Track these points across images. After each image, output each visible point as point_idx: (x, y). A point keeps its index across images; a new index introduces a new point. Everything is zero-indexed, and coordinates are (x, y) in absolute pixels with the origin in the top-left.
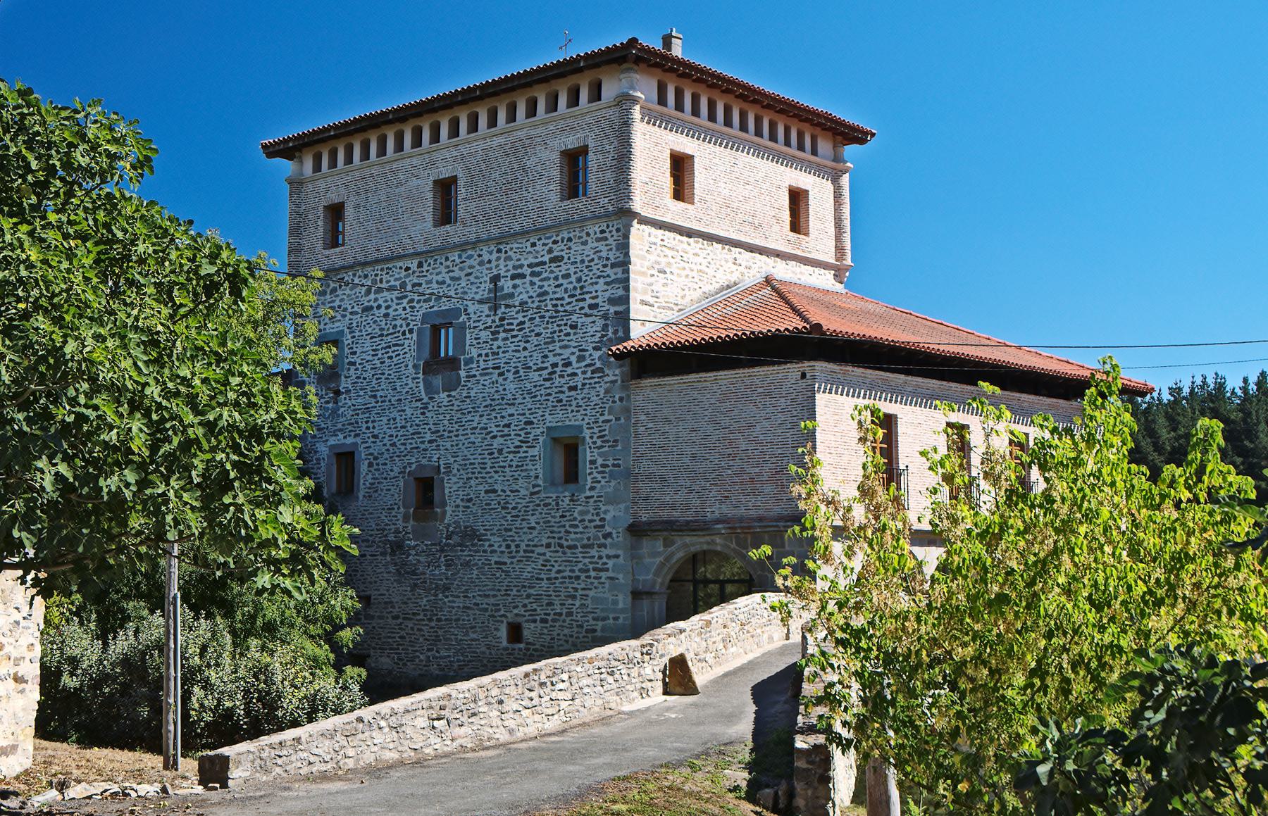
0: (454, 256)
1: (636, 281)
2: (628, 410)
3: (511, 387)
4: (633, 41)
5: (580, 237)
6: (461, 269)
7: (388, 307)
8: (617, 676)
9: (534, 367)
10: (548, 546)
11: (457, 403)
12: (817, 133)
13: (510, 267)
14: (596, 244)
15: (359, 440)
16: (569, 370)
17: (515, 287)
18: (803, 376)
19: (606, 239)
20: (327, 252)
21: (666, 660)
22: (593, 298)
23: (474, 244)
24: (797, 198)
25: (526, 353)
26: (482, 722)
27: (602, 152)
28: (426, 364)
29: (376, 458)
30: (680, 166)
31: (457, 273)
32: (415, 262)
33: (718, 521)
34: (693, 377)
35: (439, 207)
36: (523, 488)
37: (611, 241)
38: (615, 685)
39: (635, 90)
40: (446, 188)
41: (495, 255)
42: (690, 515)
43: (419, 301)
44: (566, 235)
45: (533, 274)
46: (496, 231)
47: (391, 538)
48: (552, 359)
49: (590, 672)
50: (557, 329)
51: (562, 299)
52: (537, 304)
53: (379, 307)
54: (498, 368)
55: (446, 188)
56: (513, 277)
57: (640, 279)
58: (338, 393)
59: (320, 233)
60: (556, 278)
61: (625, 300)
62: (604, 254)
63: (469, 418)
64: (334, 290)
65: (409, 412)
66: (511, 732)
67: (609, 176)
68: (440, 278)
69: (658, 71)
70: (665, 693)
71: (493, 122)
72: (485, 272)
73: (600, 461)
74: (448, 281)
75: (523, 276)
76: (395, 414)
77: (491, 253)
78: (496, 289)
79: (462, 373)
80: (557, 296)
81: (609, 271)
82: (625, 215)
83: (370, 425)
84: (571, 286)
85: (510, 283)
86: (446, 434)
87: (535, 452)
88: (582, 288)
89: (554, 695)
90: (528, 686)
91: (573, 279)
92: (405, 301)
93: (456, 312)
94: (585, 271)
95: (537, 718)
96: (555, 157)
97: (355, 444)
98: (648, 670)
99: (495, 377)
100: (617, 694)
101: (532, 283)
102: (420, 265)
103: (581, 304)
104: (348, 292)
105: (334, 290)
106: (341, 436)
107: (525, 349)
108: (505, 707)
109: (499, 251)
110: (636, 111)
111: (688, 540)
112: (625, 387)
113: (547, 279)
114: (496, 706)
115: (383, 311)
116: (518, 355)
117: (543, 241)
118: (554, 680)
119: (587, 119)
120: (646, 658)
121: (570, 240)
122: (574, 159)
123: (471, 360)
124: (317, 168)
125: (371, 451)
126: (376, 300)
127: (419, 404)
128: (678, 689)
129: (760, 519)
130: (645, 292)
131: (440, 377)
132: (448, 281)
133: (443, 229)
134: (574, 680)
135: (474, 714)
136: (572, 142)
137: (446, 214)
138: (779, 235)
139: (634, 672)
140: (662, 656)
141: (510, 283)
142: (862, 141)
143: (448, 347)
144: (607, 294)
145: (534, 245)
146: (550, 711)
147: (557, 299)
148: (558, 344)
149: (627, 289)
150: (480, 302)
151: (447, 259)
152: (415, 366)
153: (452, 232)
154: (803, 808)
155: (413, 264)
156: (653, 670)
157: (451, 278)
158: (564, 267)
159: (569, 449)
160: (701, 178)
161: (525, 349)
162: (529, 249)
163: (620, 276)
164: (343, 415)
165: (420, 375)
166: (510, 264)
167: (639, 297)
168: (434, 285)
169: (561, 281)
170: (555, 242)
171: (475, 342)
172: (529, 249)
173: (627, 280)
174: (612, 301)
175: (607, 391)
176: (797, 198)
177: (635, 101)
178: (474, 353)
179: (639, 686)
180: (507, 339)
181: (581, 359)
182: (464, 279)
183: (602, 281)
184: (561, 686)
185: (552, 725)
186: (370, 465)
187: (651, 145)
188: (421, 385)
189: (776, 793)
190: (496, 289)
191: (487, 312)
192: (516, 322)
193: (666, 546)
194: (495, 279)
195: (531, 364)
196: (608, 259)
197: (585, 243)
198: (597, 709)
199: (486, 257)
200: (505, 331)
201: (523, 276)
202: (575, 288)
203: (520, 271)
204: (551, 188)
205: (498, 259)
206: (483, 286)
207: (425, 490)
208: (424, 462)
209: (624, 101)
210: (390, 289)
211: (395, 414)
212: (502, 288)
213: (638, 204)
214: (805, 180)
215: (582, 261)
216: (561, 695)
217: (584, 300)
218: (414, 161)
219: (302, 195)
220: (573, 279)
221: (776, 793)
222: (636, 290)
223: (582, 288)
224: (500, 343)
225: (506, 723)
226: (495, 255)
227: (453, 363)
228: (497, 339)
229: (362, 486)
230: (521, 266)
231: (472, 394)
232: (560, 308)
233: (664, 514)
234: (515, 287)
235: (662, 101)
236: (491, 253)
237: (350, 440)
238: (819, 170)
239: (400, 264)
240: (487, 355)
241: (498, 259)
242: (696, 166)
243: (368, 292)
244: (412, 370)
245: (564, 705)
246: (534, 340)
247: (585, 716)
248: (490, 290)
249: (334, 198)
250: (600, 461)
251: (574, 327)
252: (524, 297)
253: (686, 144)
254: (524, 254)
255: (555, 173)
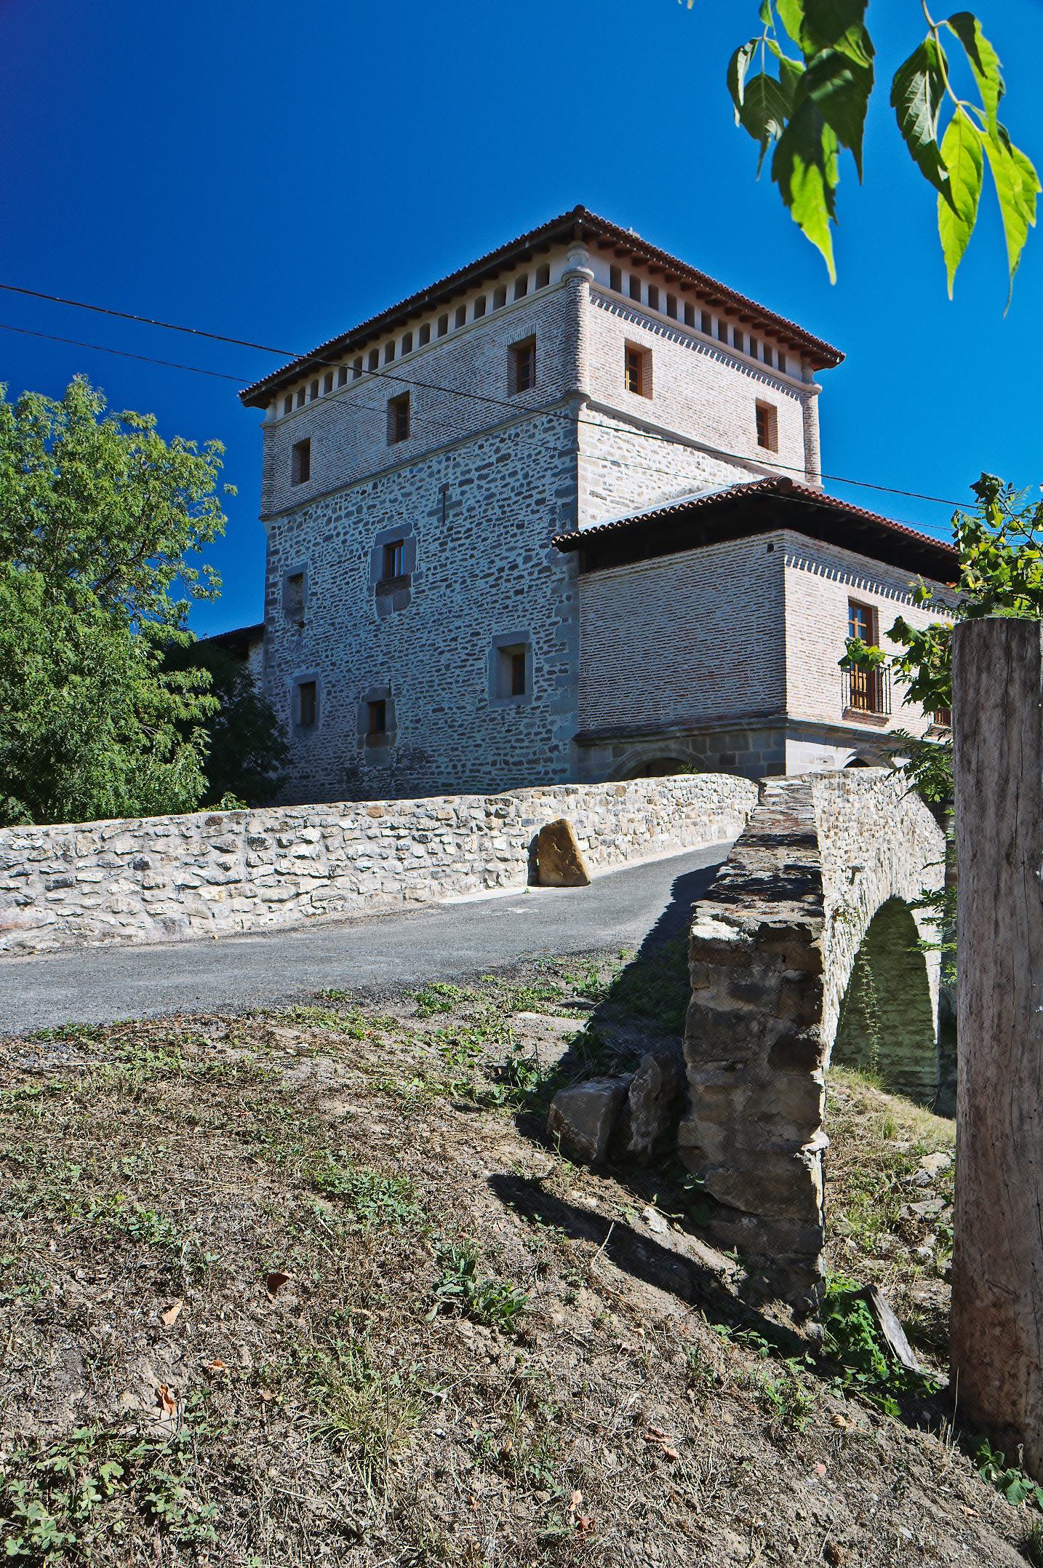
0: (406, 472)
1: (585, 469)
2: (575, 610)
3: (458, 598)
4: (580, 209)
5: (527, 431)
6: (412, 484)
7: (345, 534)
8: (435, 845)
9: (481, 575)
10: (494, 763)
11: (407, 621)
12: (786, 348)
13: (458, 474)
14: (543, 436)
15: (319, 670)
16: (516, 573)
17: (463, 493)
18: (770, 548)
19: (554, 428)
20: (294, 489)
21: (535, 830)
22: (540, 493)
23: (424, 456)
24: (765, 415)
25: (473, 561)
26: (88, 902)
27: (550, 339)
28: (380, 585)
29: (334, 686)
30: (637, 360)
31: (409, 488)
32: (371, 485)
33: (673, 724)
34: (645, 564)
35: (394, 427)
36: (469, 703)
37: (558, 429)
38: (428, 861)
39: (583, 266)
40: (400, 406)
41: (444, 464)
42: (642, 719)
43: (373, 523)
44: (513, 432)
45: (481, 477)
46: (445, 439)
47: (347, 765)
48: (499, 564)
49: (374, 831)
50: (503, 531)
51: (509, 498)
52: (484, 507)
53: (338, 534)
54: (446, 580)
55: (400, 406)
56: (461, 484)
57: (590, 468)
58: (302, 625)
59: (289, 473)
60: (503, 478)
61: (573, 490)
62: (551, 445)
63: (418, 635)
64: (301, 524)
65: (363, 636)
66: (169, 925)
67: (556, 362)
68: (392, 497)
69: (610, 253)
70: (535, 880)
71: (443, 330)
72: (435, 483)
73: (546, 668)
74: (400, 498)
75: (470, 481)
76: (351, 639)
77: (440, 463)
78: (445, 498)
79: (412, 590)
80: (504, 496)
81: (556, 461)
82: (574, 397)
83: (329, 653)
84: (518, 484)
85: (459, 490)
86: (397, 654)
87: (481, 664)
88: (529, 484)
89: (284, 865)
90: (218, 841)
91: (520, 476)
92: (361, 525)
93: (406, 529)
94: (533, 465)
95: (239, 903)
96: (502, 353)
97: (316, 674)
98: (500, 843)
99: (443, 590)
100: (434, 876)
101: (480, 487)
102: (375, 487)
103: (528, 501)
104: (311, 524)
105: (301, 524)
106: (304, 667)
107: (472, 556)
108: (152, 877)
109: (448, 459)
110: (585, 289)
111: (639, 747)
112: (573, 584)
113: (494, 480)
114: (129, 872)
115: (342, 538)
116: (465, 564)
117: (491, 441)
118: (285, 838)
119: (535, 307)
120: (496, 822)
121: (517, 435)
122: (523, 353)
123: (419, 576)
124: (288, 408)
125: (330, 678)
126: (336, 528)
127: (372, 627)
128: (554, 877)
129: (720, 718)
130: (596, 483)
131: (391, 597)
132: (400, 498)
133: (396, 446)
134: (334, 843)
135: (64, 884)
136: (519, 334)
137: (400, 431)
138: (746, 445)
139: (473, 841)
140: (527, 822)
141: (459, 490)
142: (832, 364)
143: (400, 568)
144: (555, 487)
145: (481, 447)
146: (274, 894)
147: (504, 500)
148: (505, 547)
149: (575, 478)
150: (430, 514)
151: (399, 476)
152: (369, 589)
153: (407, 448)
154: (715, 1156)
155: (368, 487)
156: (510, 843)
157: (404, 495)
158: (512, 465)
159: (514, 657)
160: (659, 374)
161: (472, 556)
162: (477, 451)
163: (568, 464)
164: (306, 646)
165: (374, 598)
166: (459, 470)
167: (590, 488)
168: (388, 504)
169: (508, 480)
170: (502, 441)
171: (424, 556)
172: (477, 451)
173: (576, 467)
174: (559, 493)
175: (554, 591)
176: (765, 415)
177: (584, 278)
178: (424, 567)
179: (479, 866)
180: (454, 549)
181: (527, 559)
182: (415, 493)
183: (549, 473)
184: (304, 849)
185: (287, 915)
186: (329, 693)
187: (603, 333)
188: (374, 606)
189: (621, 1098)
190: (445, 498)
191: (436, 524)
192: (463, 530)
193: (615, 756)
194: (444, 488)
195: (478, 572)
196: (555, 449)
197: (532, 436)
198: (387, 898)
199: (435, 468)
200: (453, 540)
201: (470, 481)
202: (522, 485)
203: (467, 476)
204: (499, 385)
205: (447, 467)
206: (432, 498)
207: (378, 712)
208: (377, 685)
209: (574, 278)
210: (348, 515)
211: (351, 639)
212: (451, 497)
213: (587, 385)
214: (774, 396)
215: (529, 456)
216: (300, 867)
217: (531, 496)
218: (371, 384)
219: (276, 439)
220: (520, 476)
221: (621, 1098)
222: (585, 479)
223: (529, 484)
224: (448, 554)
225: (157, 908)
226: (444, 464)
227: (404, 581)
228: (444, 550)
229: (321, 715)
230: (469, 471)
231: (422, 610)
232: (507, 509)
233: (614, 721)
234: (463, 493)
235: (615, 285)
236: (440, 463)
237: (311, 670)
238: (787, 388)
239: (357, 488)
240: (435, 568)
241: (447, 467)
242: (654, 360)
243: (329, 521)
244: (366, 593)
245: (307, 884)
246: (481, 546)
247: (357, 906)
248: (439, 501)
249: (301, 435)
250: (546, 668)
251: (520, 526)
252: (472, 502)
253: (645, 337)
254: (470, 458)
255: (503, 370)
